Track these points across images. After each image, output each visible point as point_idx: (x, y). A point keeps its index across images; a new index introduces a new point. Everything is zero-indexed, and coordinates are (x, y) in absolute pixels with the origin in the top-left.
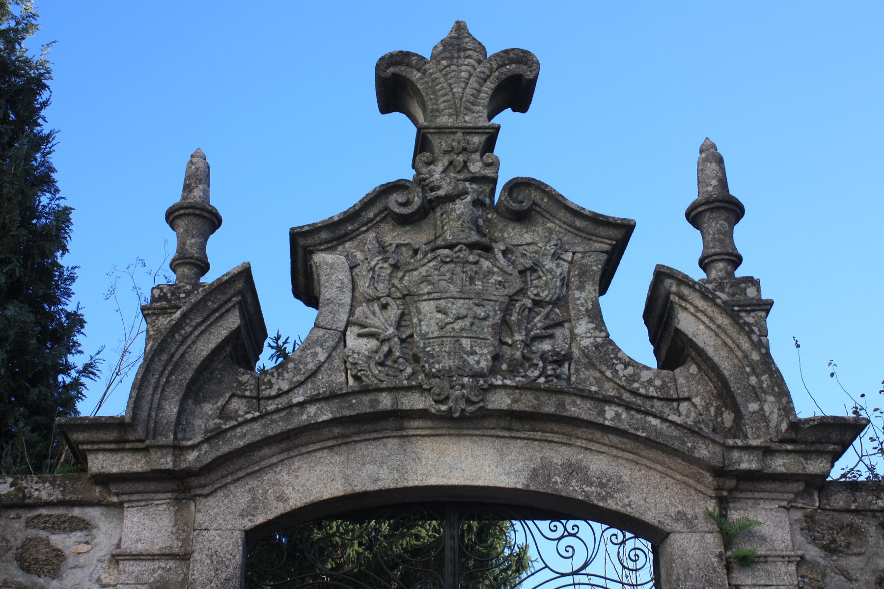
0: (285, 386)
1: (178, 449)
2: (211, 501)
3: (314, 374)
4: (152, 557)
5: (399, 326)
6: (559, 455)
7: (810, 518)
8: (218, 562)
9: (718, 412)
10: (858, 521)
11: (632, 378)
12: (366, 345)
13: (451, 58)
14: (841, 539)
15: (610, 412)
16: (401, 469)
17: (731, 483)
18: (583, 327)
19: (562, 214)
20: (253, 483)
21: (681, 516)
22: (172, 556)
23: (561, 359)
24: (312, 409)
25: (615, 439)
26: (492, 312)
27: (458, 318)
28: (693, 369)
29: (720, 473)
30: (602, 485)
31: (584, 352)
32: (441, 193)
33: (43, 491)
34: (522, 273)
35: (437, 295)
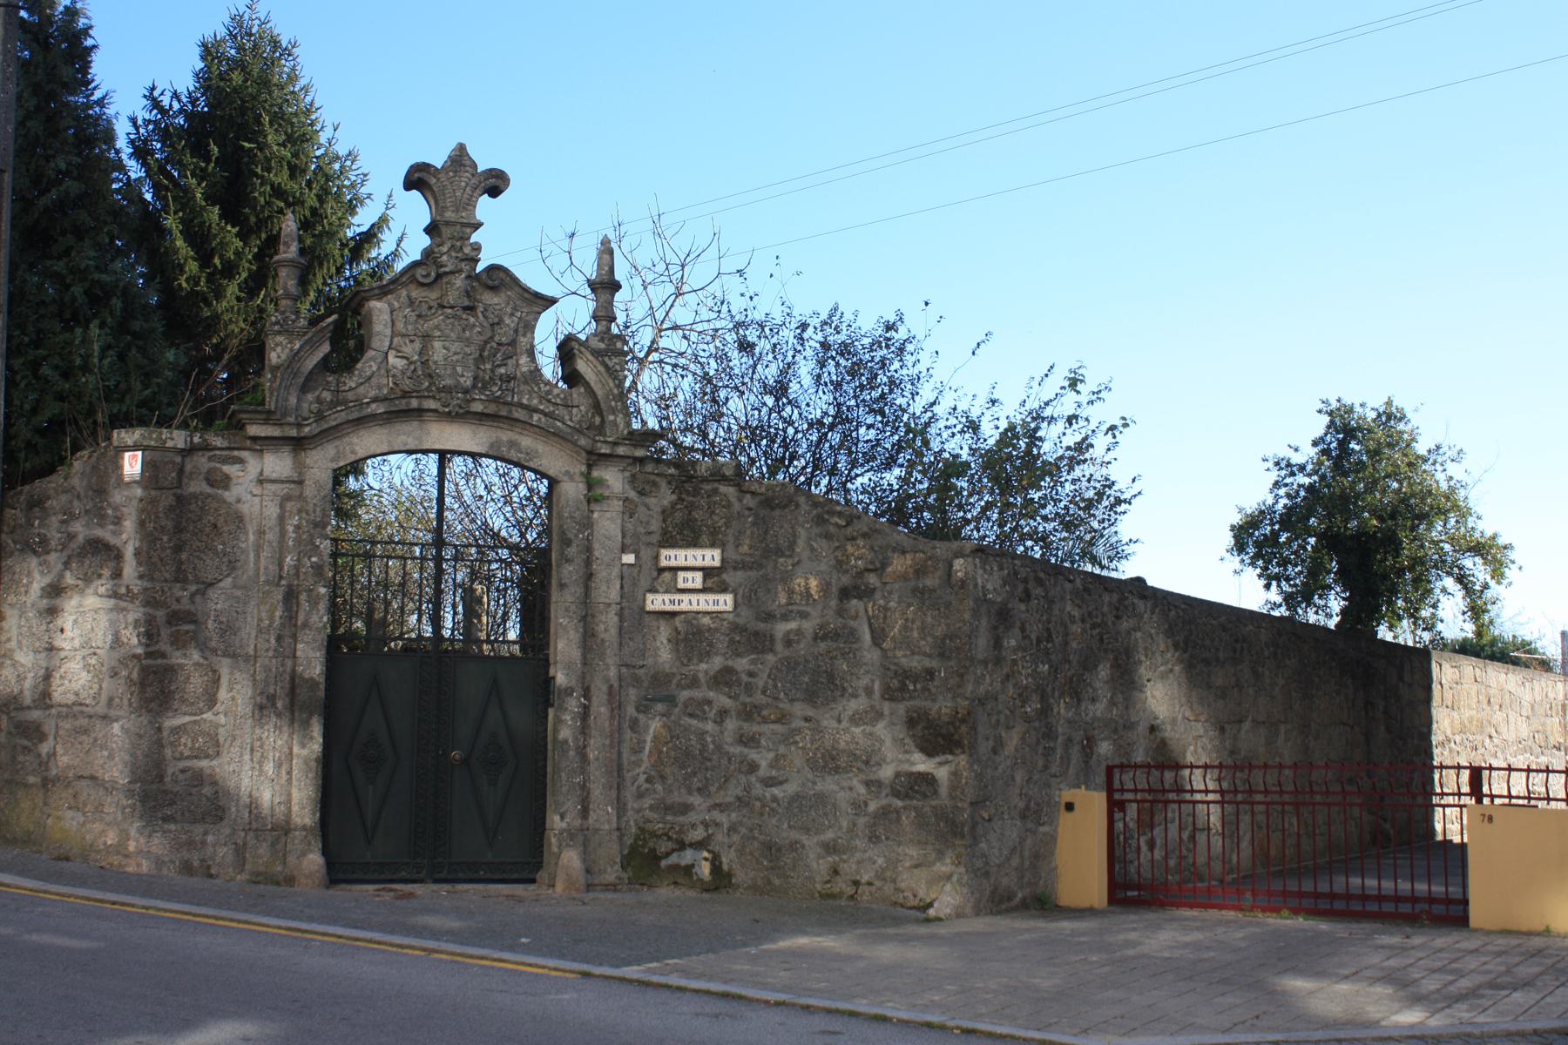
0: (354, 385)
1: (299, 426)
2: (314, 452)
3: (370, 378)
4: (282, 482)
5: (420, 354)
6: (506, 436)
7: (633, 476)
8: (319, 487)
9: (593, 416)
10: (658, 479)
11: (549, 393)
13: (455, 172)
14: (647, 488)
15: (536, 417)
16: (419, 439)
17: (595, 458)
18: (524, 360)
19: (517, 288)
20: (337, 443)
21: (567, 473)
22: (294, 482)
23: (509, 379)
24: (374, 406)
25: (537, 430)
26: (472, 350)
27: (455, 354)
28: (582, 390)
29: (590, 453)
30: (528, 454)
32: (447, 269)
33: (218, 442)
34: (492, 325)
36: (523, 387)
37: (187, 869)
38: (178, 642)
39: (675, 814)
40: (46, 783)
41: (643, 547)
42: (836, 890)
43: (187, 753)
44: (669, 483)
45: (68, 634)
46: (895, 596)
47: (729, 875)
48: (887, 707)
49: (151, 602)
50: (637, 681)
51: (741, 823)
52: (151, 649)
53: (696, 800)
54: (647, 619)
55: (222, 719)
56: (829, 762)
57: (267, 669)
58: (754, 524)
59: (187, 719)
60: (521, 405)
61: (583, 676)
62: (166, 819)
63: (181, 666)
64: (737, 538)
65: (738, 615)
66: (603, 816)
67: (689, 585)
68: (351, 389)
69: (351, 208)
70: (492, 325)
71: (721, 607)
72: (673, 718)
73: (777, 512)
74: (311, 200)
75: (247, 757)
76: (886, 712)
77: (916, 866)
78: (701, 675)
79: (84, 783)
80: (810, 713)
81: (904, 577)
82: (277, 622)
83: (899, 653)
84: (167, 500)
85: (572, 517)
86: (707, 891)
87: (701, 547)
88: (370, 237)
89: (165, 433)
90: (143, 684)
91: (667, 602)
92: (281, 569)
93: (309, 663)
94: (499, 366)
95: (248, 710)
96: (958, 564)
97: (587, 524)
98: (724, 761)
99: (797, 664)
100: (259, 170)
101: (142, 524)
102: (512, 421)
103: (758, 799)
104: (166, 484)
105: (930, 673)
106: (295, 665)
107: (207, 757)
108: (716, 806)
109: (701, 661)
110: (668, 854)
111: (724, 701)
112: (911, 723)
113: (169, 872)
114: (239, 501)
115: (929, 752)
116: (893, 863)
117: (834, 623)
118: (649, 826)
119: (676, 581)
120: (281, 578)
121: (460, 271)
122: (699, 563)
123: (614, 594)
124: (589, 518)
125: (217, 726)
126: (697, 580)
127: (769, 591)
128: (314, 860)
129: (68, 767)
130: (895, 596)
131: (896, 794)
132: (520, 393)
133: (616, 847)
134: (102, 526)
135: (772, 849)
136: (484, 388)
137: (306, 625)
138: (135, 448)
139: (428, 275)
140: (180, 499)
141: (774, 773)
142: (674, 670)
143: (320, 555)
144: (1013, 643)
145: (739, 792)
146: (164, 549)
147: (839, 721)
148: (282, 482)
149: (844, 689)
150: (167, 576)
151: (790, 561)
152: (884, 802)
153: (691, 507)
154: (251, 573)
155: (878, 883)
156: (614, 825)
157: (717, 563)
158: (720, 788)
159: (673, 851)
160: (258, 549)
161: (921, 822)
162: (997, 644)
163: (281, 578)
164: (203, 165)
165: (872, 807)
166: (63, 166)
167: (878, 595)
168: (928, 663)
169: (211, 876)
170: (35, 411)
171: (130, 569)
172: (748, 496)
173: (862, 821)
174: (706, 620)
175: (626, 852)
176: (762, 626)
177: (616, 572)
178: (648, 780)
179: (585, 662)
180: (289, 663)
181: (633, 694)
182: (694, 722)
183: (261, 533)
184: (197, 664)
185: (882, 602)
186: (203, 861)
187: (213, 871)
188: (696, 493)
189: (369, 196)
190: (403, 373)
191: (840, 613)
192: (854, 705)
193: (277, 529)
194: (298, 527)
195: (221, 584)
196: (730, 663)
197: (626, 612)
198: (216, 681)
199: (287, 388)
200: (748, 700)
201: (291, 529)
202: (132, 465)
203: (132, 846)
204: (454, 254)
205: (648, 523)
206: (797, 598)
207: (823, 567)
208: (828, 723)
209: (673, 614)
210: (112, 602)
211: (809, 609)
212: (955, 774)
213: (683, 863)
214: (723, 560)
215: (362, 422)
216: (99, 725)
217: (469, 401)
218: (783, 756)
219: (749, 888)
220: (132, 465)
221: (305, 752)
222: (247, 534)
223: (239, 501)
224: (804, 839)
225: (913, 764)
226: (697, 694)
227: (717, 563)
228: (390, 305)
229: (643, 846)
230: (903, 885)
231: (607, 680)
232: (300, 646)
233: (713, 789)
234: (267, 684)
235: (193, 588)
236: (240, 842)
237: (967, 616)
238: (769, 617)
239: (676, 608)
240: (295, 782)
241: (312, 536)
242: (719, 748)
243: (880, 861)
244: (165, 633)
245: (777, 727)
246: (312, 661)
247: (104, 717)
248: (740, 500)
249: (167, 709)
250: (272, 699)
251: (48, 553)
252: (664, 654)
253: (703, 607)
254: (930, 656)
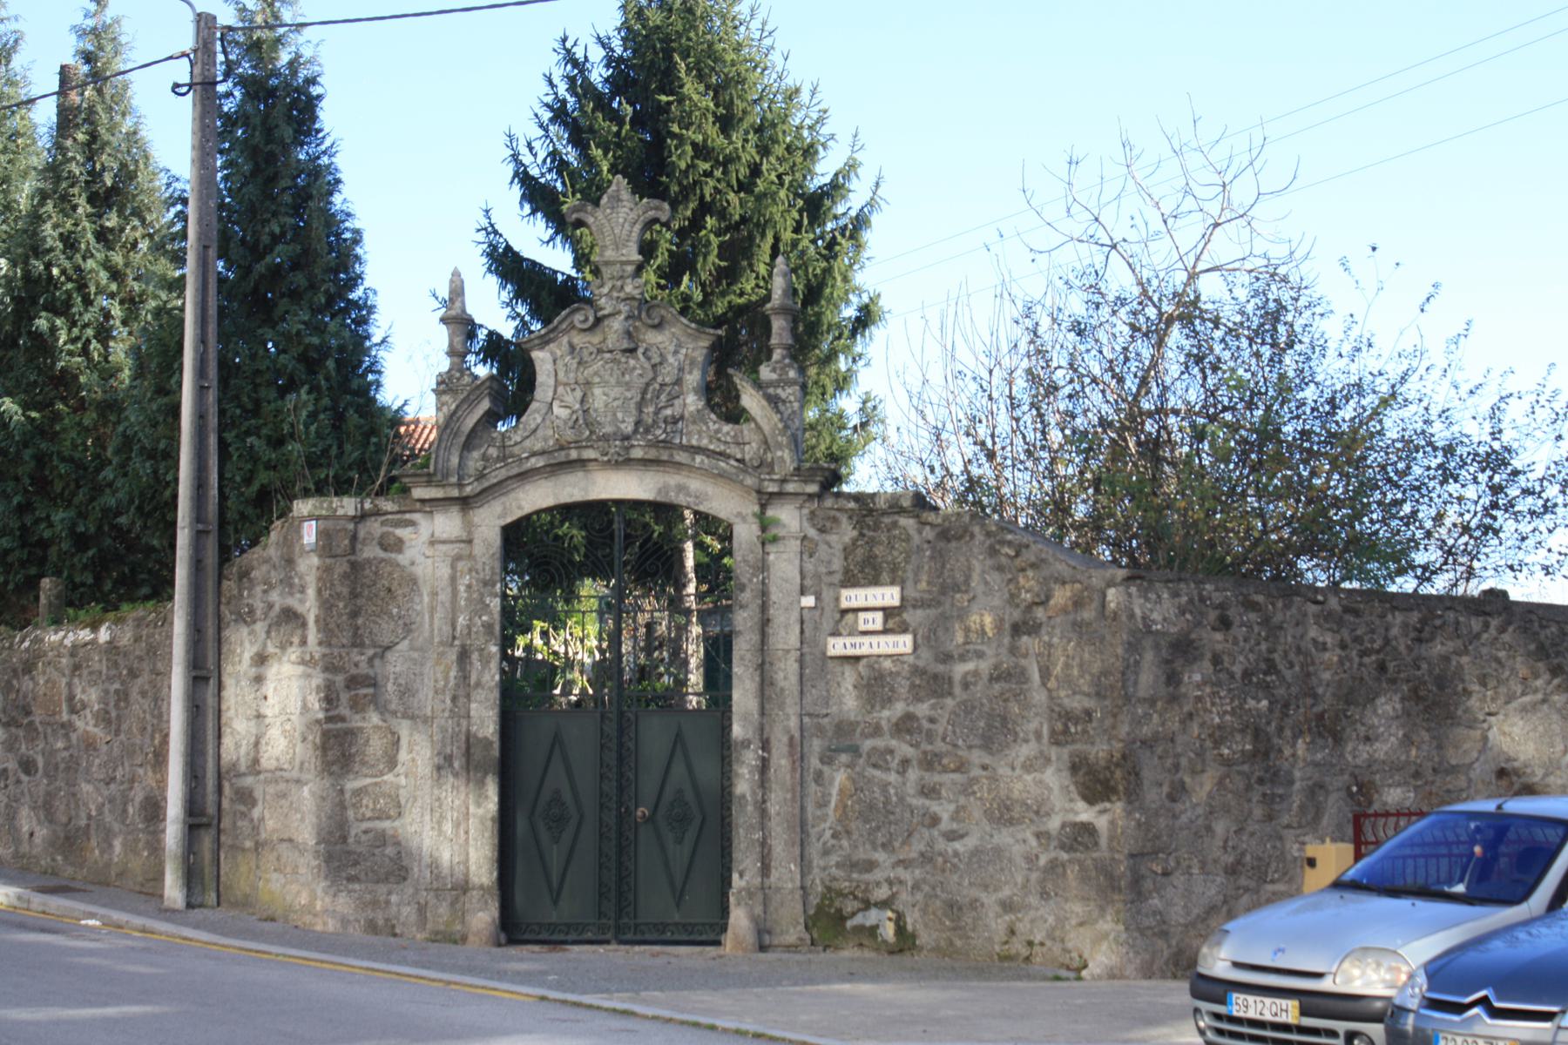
3: (535, 431)
4: (452, 542)
5: (582, 401)
6: (673, 479)
7: (812, 513)
8: (489, 545)
10: (838, 514)
14: (828, 525)
15: (698, 459)
20: (503, 499)
21: (739, 514)
23: (675, 420)
24: (533, 460)
26: (634, 395)
31: (691, 413)
32: (605, 312)
33: (387, 505)
34: (654, 366)
35: (604, 383)
36: (691, 427)
37: (372, 927)
38: (357, 706)
39: (860, 872)
40: (258, 846)
41: (824, 588)
42: (1013, 952)
43: (369, 814)
44: (850, 518)
45: (271, 701)
46: (1058, 631)
47: (914, 936)
48: (1053, 752)
49: (330, 668)
50: (821, 730)
51: (924, 880)
53: (880, 856)
54: (830, 664)
55: (403, 781)
56: (1004, 814)
57: (443, 730)
58: (932, 558)
59: (368, 781)
60: (682, 447)
61: (762, 729)
62: (351, 879)
63: (361, 729)
64: (916, 574)
65: (918, 657)
66: (786, 873)
67: (870, 627)
68: (516, 444)
69: (810, 152)
70: (654, 366)
71: (901, 650)
72: (857, 769)
73: (954, 544)
74: (750, 154)
75: (427, 818)
76: (1054, 758)
77: (1081, 924)
78: (884, 723)
79: (285, 845)
80: (987, 760)
81: (1065, 611)
82: (452, 683)
83: (1062, 693)
84: (342, 567)
85: (745, 561)
86: (891, 953)
87: (882, 585)
88: (835, 188)
89: (336, 501)
90: (324, 748)
92: (454, 629)
93: (483, 722)
94: (665, 407)
95: (428, 771)
96: (1112, 593)
97: (763, 567)
98: (907, 815)
99: (974, 708)
100: (675, 128)
101: (319, 591)
102: (679, 466)
103: (940, 854)
104: (339, 551)
105: (1088, 713)
106: (469, 725)
107: (388, 818)
108: (900, 862)
109: (883, 708)
110: (854, 914)
111: (904, 749)
112: (1074, 768)
113: (356, 932)
114: (413, 563)
115: (1090, 798)
116: (1061, 921)
117: (1007, 662)
118: (835, 885)
119: (856, 621)
120: (454, 638)
121: (619, 312)
122: (879, 603)
123: (793, 639)
124: (764, 560)
125: (398, 787)
126: (876, 621)
127: (947, 630)
128: (484, 917)
129: (275, 831)
130: (1058, 631)
131: (1063, 847)
132: (689, 434)
133: (799, 907)
134: (291, 594)
135: (953, 907)
136: (647, 431)
137: (478, 684)
138: (310, 517)
139: (586, 319)
140: (354, 566)
141: (955, 826)
142: (859, 718)
143: (491, 613)
144: (1197, 677)
145: (922, 847)
146: (340, 615)
147: (1013, 769)
148: (452, 542)
149: (1016, 734)
150: (345, 641)
151: (966, 597)
152: (1053, 855)
153: (872, 542)
154: (427, 634)
155: (1049, 943)
156: (798, 884)
157: (896, 602)
158: (904, 843)
159: (859, 910)
160: (432, 610)
161: (1084, 878)
162: (1173, 679)
163: (454, 638)
164: (615, 129)
165: (1043, 861)
166: (277, 230)
167: (1043, 631)
168: (1089, 703)
169: (395, 935)
170: (248, 481)
171: (313, 635)
172: (928, 528)
173: (1034, 876)
174: (887, 664)
175: (812, 912)
176: (941, 668)
177: (795, 616)
178: (834, 836)
179: (763, 713)
180: (464, 723)
181: (816, 745)
182: (877, 773)
183: (434, 594)
184: (377, 727)
185: (1046, 638)
186: (387, 920)
187: (398, 931)
188: (876, 528)
189: (832, 137)
190: (565, 422)
191: (1013, 650)
192: (1026, 751)
193: (449, 590)
194: (469, 587)
195: (399, 647)
196: (911, 709)
197: (808, 658)
198: (396, 743)
199: (448, 449)
200: (929, 748)
201: (462, 588)
202: (309, 534)
203: (319, 905)
204: (615, 294)
205: (829, 562)
206: (973, 636)
207: (997, 602)
208: (1003, 770)
209: (857, 659)
210: (301, 669)
211: (984, 648)
212: (1112, 823)
213: (868, 924)
214: (903, 599)
215: (524, 476)
216: (294, 788)
217: (628, 449)
218: (964, 808)
219: (932, 950)
220: (309, 534)
221: (481, 811)
222: (421, 595)
223: (413, 563)
224: (983, 896)
225: (1077, 813)
226: (880, 743)
227: (896, 602)
228: (552, 353)
229: (830, 906)
230: (1070, 945)
231: (787, 730)
232: (473, 706)
233: (897, 844)
234: (444, 746)
235: (370, 652)
236: (422, 901)
237: (1120, 651)
238: (947, 658)
239: (858, 652)
240: (471, 842)
241: (482, 595)
242: (901, 799)
243: (1051, 919)
244: (344, 697)
245: (956, 777)
246: (485, 720)
247: (298, 781)
248: (920, 532)
249: (348, 772)
250: (449, 759)
251: (254, 622)
252: (848, 700)
253: (884, 650)
254: (1088, 695)
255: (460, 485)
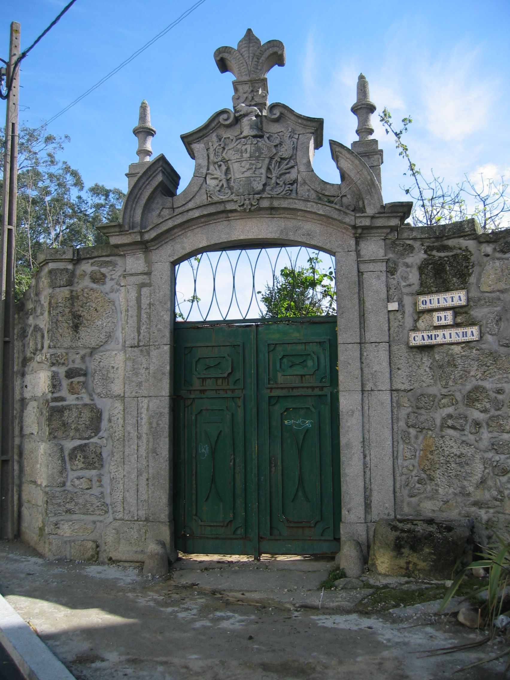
6: (290, 224)
12: (214, 182)
25: (313, 216)
32: (242, 113)
52: (56, 395)
67: (443, 322)
71: (469, 338)
91: (426, 337)
122: (449, 304)
126: (448, 317)
157: (463, 302)
214: (468, 299)
239: (434, 342)
244: (65, 383)
255: (142, 234)
